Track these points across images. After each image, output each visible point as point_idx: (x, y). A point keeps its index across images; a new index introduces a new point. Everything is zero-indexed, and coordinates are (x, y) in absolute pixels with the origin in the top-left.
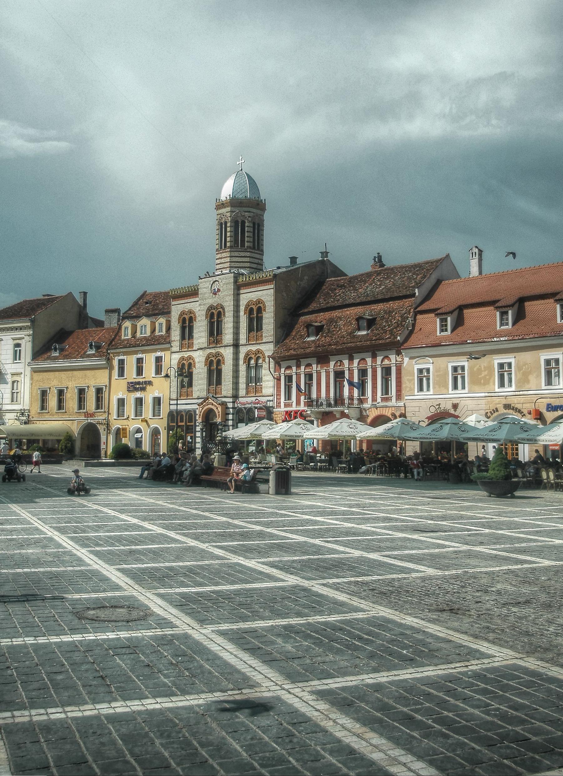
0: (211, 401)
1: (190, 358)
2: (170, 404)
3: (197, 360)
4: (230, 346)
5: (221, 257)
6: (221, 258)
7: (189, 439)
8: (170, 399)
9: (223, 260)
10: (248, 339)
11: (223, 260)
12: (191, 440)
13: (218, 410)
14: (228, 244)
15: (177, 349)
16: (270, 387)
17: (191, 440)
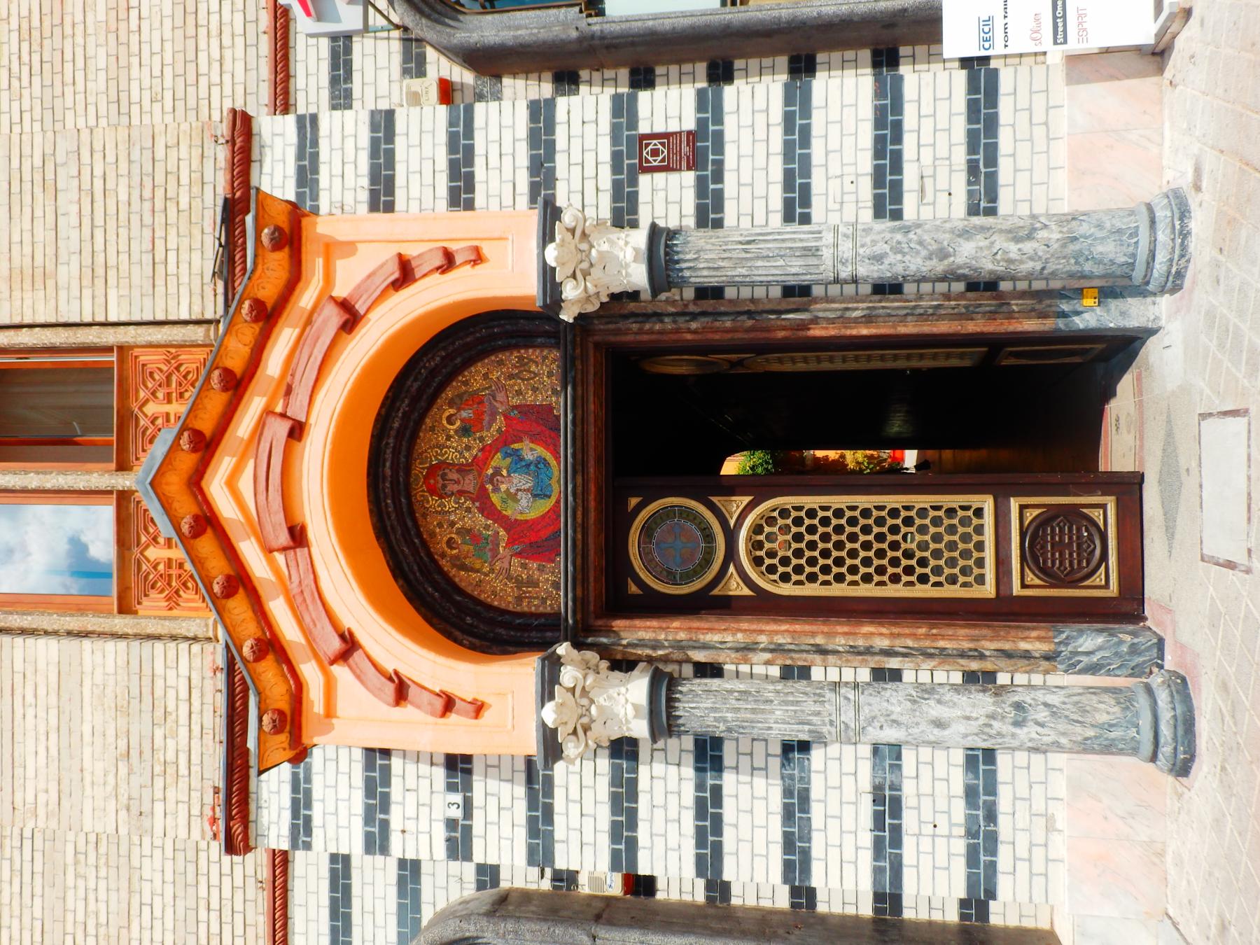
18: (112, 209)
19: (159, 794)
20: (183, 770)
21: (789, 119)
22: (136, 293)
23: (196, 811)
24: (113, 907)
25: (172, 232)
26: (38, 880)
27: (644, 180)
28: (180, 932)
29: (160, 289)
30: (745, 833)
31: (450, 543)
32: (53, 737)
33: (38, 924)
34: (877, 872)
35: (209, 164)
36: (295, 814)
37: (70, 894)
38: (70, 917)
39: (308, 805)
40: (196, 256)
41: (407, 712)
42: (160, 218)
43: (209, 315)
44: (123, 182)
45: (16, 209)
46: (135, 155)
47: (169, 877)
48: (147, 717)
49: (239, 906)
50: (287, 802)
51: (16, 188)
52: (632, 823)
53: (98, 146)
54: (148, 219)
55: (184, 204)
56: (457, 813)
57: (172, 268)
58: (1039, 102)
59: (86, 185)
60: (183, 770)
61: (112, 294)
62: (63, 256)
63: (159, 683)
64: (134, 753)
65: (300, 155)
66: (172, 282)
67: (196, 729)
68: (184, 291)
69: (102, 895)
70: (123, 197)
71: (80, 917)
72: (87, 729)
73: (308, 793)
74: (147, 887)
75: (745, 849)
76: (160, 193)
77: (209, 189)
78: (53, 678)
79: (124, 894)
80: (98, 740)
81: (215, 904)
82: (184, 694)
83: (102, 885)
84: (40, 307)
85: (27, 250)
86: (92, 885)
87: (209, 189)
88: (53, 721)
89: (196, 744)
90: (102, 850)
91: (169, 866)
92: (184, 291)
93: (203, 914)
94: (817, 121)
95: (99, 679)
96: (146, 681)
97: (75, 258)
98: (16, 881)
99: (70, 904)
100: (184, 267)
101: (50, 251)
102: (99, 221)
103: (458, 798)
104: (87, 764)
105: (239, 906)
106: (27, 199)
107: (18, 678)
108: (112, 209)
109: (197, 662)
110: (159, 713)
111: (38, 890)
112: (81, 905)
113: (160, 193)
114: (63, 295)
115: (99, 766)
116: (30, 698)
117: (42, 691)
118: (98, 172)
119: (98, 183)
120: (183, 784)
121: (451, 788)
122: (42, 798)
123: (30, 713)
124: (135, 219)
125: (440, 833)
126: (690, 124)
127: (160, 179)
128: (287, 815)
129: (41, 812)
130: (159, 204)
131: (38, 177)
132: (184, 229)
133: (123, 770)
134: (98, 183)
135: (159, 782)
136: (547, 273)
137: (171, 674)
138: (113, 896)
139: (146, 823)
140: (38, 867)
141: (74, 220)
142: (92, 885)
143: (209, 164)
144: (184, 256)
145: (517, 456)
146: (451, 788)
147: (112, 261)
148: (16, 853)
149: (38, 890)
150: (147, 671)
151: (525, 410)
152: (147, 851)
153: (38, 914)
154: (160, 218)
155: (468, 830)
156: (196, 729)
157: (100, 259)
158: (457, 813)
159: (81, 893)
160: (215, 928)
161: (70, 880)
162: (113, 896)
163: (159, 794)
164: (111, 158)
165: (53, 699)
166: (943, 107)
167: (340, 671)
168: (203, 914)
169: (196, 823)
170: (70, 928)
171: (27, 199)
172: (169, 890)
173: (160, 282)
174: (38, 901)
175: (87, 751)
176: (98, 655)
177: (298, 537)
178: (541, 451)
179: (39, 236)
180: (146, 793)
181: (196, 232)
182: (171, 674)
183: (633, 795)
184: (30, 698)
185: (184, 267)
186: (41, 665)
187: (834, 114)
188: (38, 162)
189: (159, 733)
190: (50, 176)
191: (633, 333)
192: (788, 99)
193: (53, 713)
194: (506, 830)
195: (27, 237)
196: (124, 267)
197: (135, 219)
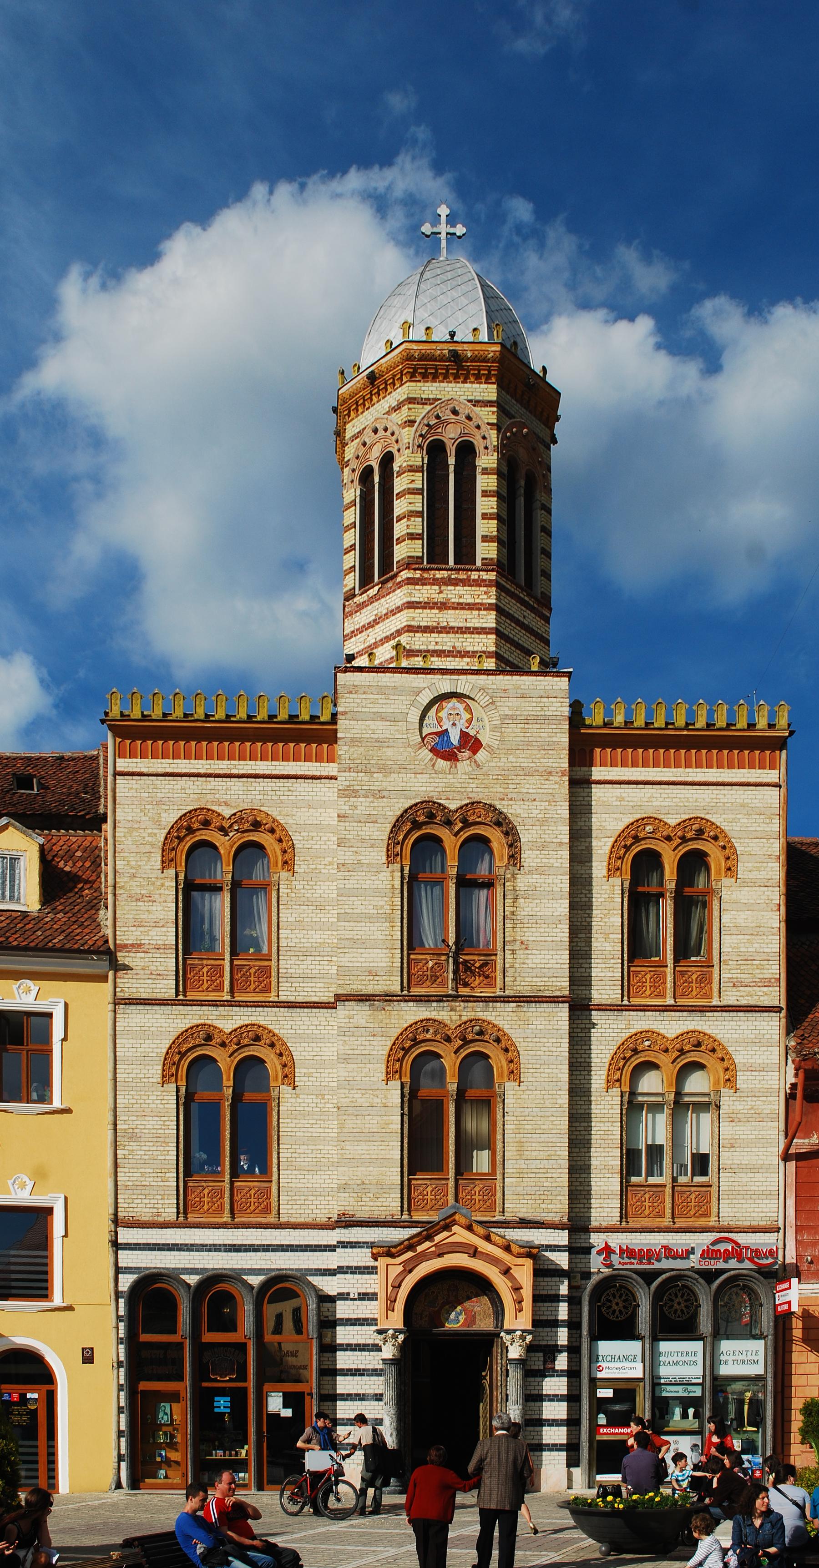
0: (460, 1234)
1: (257, 1038)
2: (116, 1245)
3: (299, 1052)
4: (553, 1000)
5: (441, 598)
6: (443, 606)
7: (275, 1403)
8: (116, 1221)
9: (452, 618)
10: (627, 986)
11: (452, 618)
12: (287, 1413)
13: (512, 1279)
14: (486, 551)
15: (166, 988)
16: (767, 1195)
17: (287, 1413)
18: (541, 1180)
19: (351, 1195)
20: (360, 1204)
21: (556, 1396)
22: (514, 1188)
23: (347, 1208)
24: (302, 1164)
25: (533, 1202)
26: (310, 1134)
27: (541, 1354)
28: (296, 1190)
29: (515, 1197)
30: (351, 1383)
31: (433, 1292)
32: (368, 1156)
33: (294, 1134)
34: (343, 1419)
35: (554, 1215)
36: (348, 1243)
37: (306, 1147)
38: (297, 1147)
39: (351, 1247)
40: (525, 1210)
41: (390, 1289)
42: (538, 1197)
43: (506, 1214)
44: (550, 1184)
45: (543, 1144)
46: (558, 1189)
47: (314, 1185)
48: (376, 1191)
49: (306, 1211)
50: (351, 1240)
51: (550, 1144)
52: (352, 1350)
53: (562, 1175)
54: (537, 1193)
55: (542, 1206)
56: (352, 1296)
57: (521, 1201)
58: (557, 1462)
59: (549, 1171)
60: (360, 1204)
61: (514, 1180)
62: (527, 1162)
63: (387, 1195)
64: (364, 1186)
65: (556, 1246)
66: (517, 1201)
67: (373, 1208)
68: (514, 1206)
69: (306, 1160)
70: (545, 1184)
71: (298, 1151)
72: (371, 1169)
73: (355, 1247)
74: (310, 1177)
75: (347, 1383)
76: (546, 1197)
77: (546, 1215)
78: (388, 1157)
79: (307, 1168)
80: (367, 1173)
81: (306, 1202)
82: (384, 1204)
83: (310, 1160)
84: (510, 1153)
85: (529, 1149)
86: (310, 1156)
87: (546, 1215)
88: (373, 1156)
89: (368, 1208)
90: (322, 1160)
91: (318, 1185)
92: (514, 1206)
93: (303, 1198)
94: (556, 1403)
95: (388, 1173)
96: (388, 1191)
97: (526, 1166)
98: (308, 1126)
99: (302, 1147)
100: (522, 1206)
101: (529, 1157)
102: (538, 1175)
103: (356, 1297)
104: (360, 1169)
105: (306, 1211)
106: (546, 1149)
107: (387, 1143)
108: (541, 1180)
109: (395, 1209)
110: (378, 1195)
111: (306, 1134)
112: (302, 1151)
113: (546, 1197)
114: (514, 1162)
115: (359, 1174)
116: (381, 1148)
117: (383, 1152)
118: (554, 1175)
119: (550, 1175)
120: (355, 1203)
121: (359, 1294)
122: (348, 1152)
123: (376, 1148)
124: (538, 1188)
125: (345, 1291)
126: (557, 1368)
127: (550, 1197)
128: (348, 1240)
129: (343, 1152)
130: (542, 1197)
131: (553, 1153)
132: (534, 1206)
133: (359, 1182)
134: (550, 1175)
135: (355, 1195)
136: (514, 1331)
137: (390, 1200)
138: (306, 1164)
139: (342, 1190)
140: (314, 1134)
141: (539, 1166)
142: (310, 1156)
143: (554, 1215)
144: (525, 1206)
145: (460, 1314)
146: (359, 1294)
147: (525, 1180)
148: (318, 1126)
149: (306, 1134)
150: (391, 1191)
151: (474, 1316)
152: (323, 1177)
153: (298, 1134)
154: (538, 1197)
155: (347, 1299)
156: (373, 1208)
157: (526, 1176)
158: (352, 1296)
159: (306, 1151)
160: (298, 1202)
161: (310, 1147)
162: (306, 1164)
163: (351, 1195)
164: (558, 1180)
165: (381, 1157)
166: (557, 1437)
167: (400, 1268)
168: (303, 1198)
169: (343, 1208)
170: (294, 1147)
171: (546, 1149)
172: (310, 1185)
173: (517, 1197)
174: (302, 1134)
175: (364, 1169)
176: (395, 1174)
177: (441, 1255)
178: (462, 1321)
179: (534, 1153)
180: (351, 1190)
181: (533, 1210)
182: (390, 1200)
183: (360, 1350)
184: (381, 1148)
185: (522, 1206)
186: (391, 1152)
187: (557, 1408)
188: (558, 1153)
189: (371, 1195)
190: (553, 1157)
191: (496, 1350)
192: (561, 1395)
193: (376, 1157)
194: (347, 1312)
195: (533, 1148)
196: (522, 1184)
197: (538, 1188)
